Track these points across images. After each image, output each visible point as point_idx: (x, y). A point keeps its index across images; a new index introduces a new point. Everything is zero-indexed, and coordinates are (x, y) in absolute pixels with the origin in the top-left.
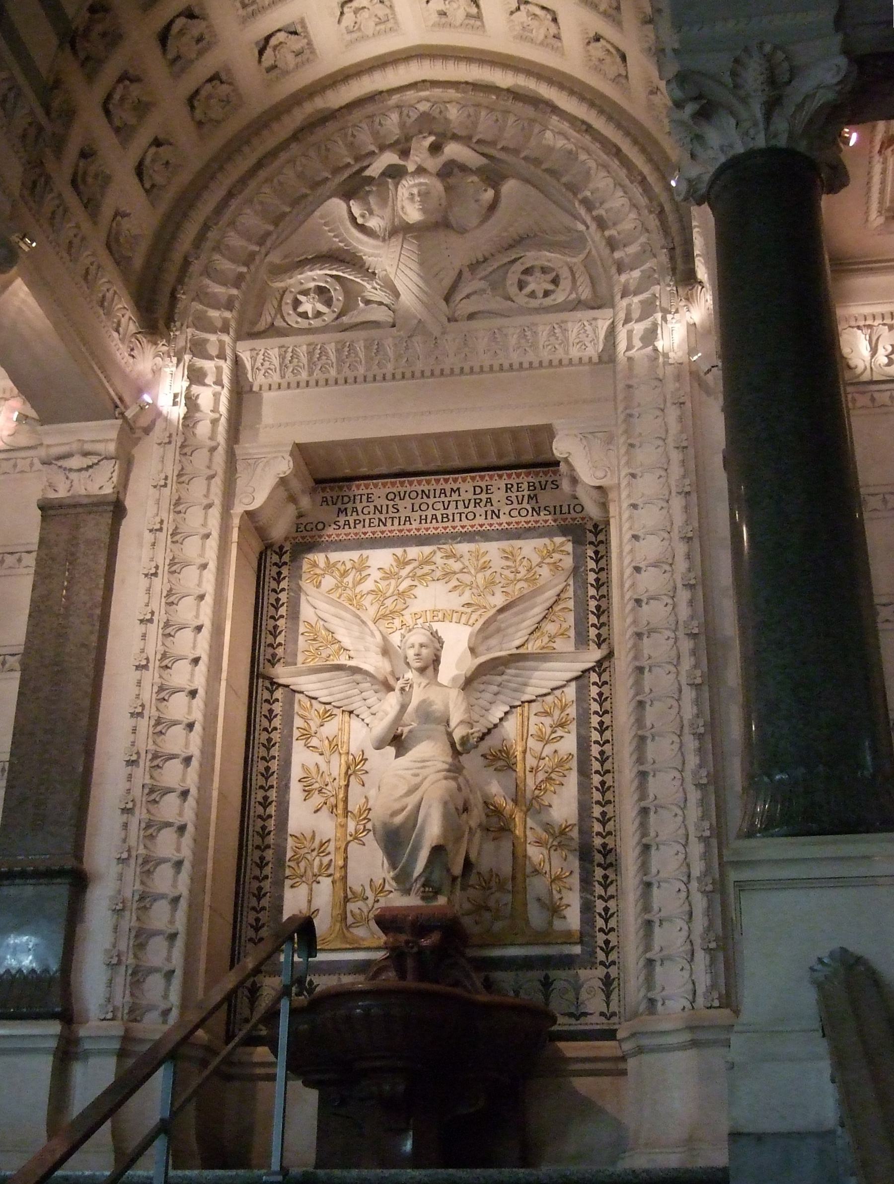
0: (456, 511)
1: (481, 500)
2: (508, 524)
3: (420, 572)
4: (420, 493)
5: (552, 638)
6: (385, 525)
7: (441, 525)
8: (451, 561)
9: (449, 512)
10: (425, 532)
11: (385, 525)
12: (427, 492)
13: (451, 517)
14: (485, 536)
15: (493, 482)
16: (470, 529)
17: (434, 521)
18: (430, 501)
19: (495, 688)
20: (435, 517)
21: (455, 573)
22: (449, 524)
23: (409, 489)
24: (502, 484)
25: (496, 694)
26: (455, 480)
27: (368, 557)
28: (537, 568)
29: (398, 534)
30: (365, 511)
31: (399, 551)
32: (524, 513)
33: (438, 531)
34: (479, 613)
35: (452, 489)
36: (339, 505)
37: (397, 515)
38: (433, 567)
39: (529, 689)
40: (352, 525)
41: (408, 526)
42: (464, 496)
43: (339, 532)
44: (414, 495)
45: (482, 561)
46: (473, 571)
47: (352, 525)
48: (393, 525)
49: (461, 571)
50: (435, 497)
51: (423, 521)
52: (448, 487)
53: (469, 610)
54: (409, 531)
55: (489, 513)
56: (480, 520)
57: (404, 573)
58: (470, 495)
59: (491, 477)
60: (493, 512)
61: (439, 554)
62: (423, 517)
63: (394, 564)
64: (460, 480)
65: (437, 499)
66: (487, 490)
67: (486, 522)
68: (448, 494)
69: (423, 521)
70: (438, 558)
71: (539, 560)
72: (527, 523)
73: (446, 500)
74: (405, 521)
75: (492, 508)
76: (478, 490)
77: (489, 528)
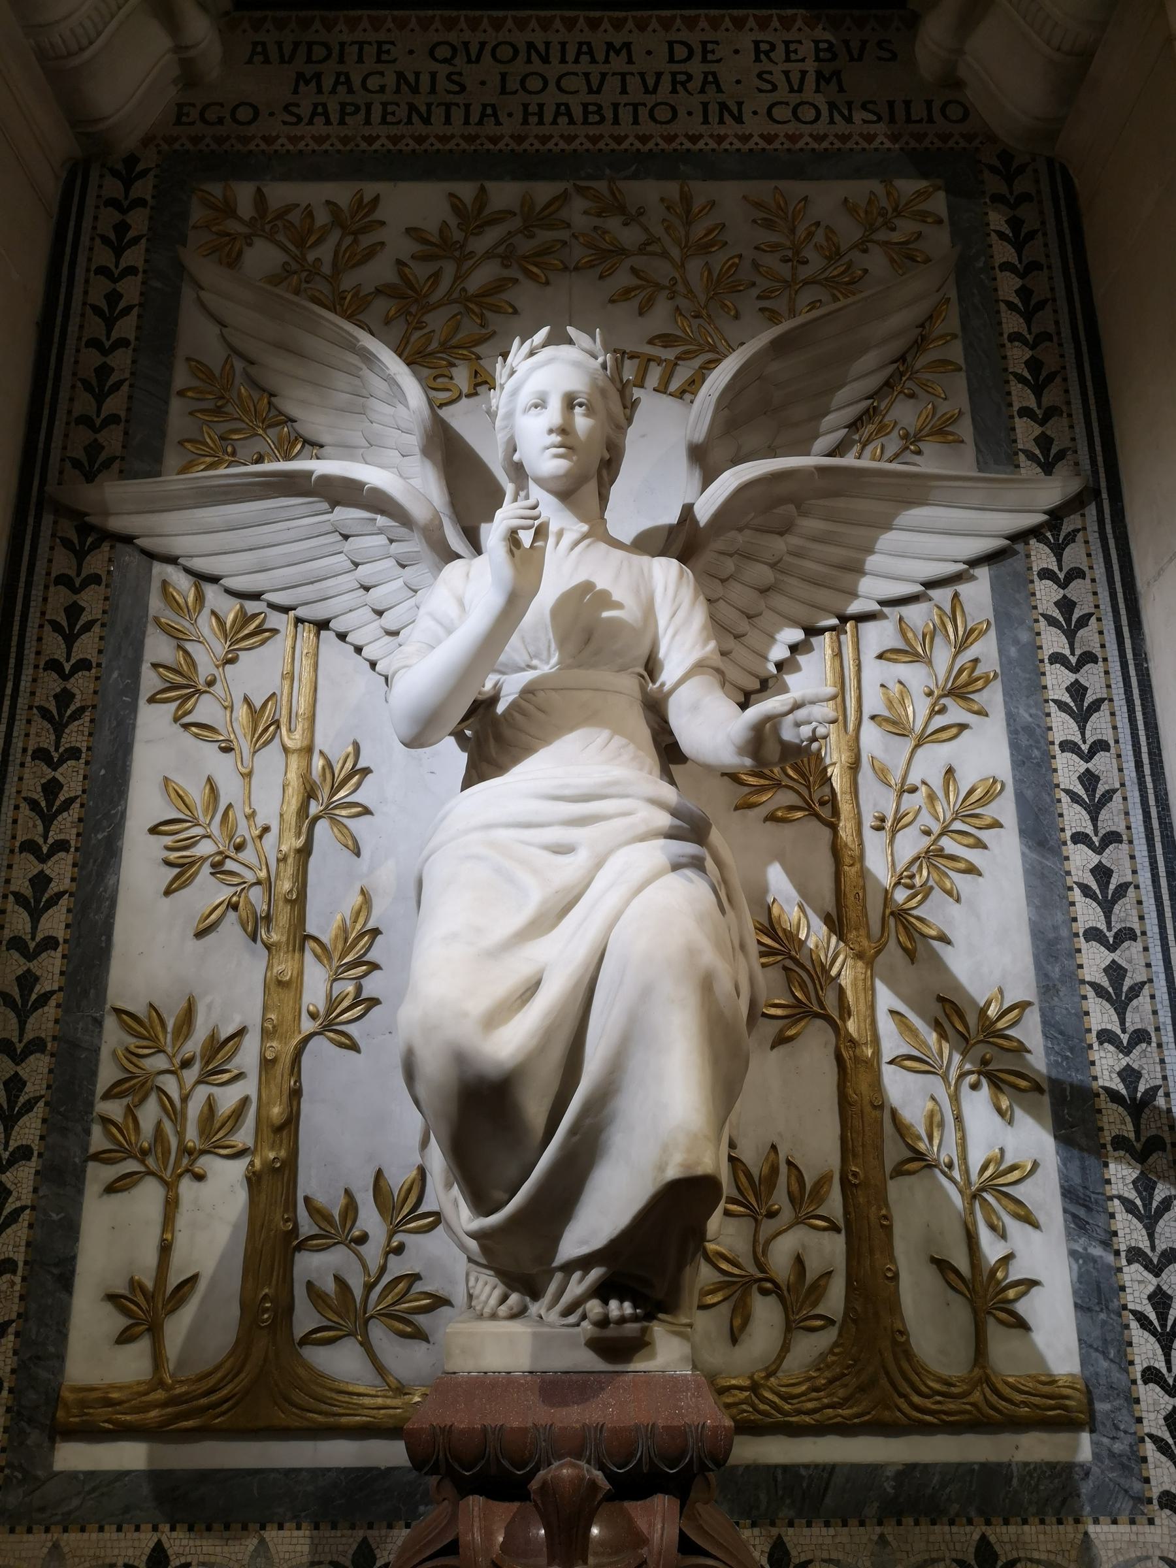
0: (624, 99)
1: (690, 77)
2: (769, 139)
3: (526, 246)
4: (523, 49)
6: (426, 121)
8: (613, 224)
10: (537, 145)
11: (426, 121)
12: (541, 48)
13: (609, 115)
16: (663, 145)
17: (563, 120)
18: (554, 69)
24: (745, 41)
26: (618, 25)
27: (376, 200)
28: (856, 255)
29: (464, 145)
30: (373, 83)
31: (466, 190)
32: (808, 114)
33: (575, 145)
34: (697, 362)
35: (610, 45)
38: (564, 235)
40: (334, 117)
43: (297, 131)
44: (505, 52)
46: (675, 253)
47: (334, 117)
48: (448, 121)
49: (642, 249)
50: (563, 61)
51: (534, 119)
53: (669, 354)
54: (494, 140)
55: (713, 109)
57: (482, 243)
59: (715, 24)
60: (723, 106)
61: (579, 204)
62: (533, 108)
63: (453, 222)
65: (571, 67)
66: (705, 52)
67: (703, 129)
68: (600, 56)
69: (534, 119)
70: (578, 213)
72: (819, 139)
74: (483, 115)
75: (721, 97)
76: (681, 52)
77: (713, 145)
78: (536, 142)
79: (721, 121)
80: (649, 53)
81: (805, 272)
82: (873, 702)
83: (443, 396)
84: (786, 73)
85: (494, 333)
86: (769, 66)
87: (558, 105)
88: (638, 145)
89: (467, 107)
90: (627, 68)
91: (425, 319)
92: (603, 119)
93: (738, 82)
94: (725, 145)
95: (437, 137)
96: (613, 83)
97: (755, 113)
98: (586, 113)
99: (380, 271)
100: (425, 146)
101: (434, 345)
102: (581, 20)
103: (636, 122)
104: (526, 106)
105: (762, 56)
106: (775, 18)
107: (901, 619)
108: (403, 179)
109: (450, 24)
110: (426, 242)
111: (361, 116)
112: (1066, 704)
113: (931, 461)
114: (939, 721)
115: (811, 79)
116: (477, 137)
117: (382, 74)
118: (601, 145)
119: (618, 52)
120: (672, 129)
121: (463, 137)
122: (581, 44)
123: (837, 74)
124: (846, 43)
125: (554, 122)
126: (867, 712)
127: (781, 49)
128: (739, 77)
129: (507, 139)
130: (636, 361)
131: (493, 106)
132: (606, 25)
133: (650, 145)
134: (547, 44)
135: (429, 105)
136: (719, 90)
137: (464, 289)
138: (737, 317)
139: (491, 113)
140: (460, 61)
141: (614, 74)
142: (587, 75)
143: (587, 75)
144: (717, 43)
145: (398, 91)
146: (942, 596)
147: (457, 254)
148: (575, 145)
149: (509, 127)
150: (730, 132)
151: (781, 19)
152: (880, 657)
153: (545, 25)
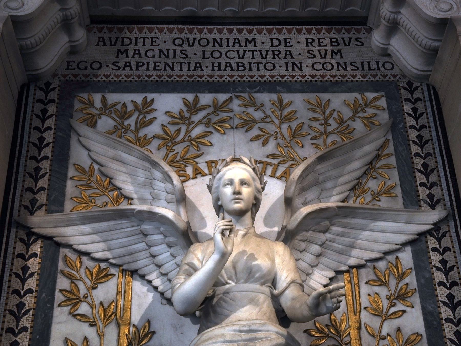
1: (280, 52)
2: (313, 77)
3: (215, 119)
4: (211, 41)
5: (376, 196)
6: (172, 69)
7: (236, 73)
8: (251, 110)
10: (218, 79)
11: (172, 69)
12: (219, 41)
13: (247, 67)
15: (292, 36)
16: (270, 79)
17: (229, 69)
18: (224, 49)
19: (315, 248)
20: (228, 65)
21: (256, 122)
22: (246, 73)
23: (198, 36)
25: (318, 256)
26: (250, 32)
27: (153, 100)
28: (350, 122)
29: (188, 79)
30: (150, 54)
31: (190, 97)
33: (234, 79)
34: (287, 165)
35: (247, 40)
36: (119, 46)
37: (186, 61)
38: (230, 114)
39: (356, 252)
40: (134, 67)
41: (199, 72)
42: (260, 46)
43: (118, 73)
44: (204, 42)
45: (286, 111)
46: (277, 122)
47: (134, 67)
48: (181, 69)
49: (263, 120)
50: (228, 46)
51: (216, 69)
52: (242, 37)
53: (275, 162)
54: (201, 77)
55: (290, 64)
56: (283, 71)
57: (196, 118)
58: (267, 46)
59: (289, 31)
60: (294, 64)
61: (236, 103)
62: (216, 64)
63: (185, 109)
64: (255, 31)
67: (286, 73)
68: (243, 44)
69: (216, 69)
70: (236, 105)
71: (351, 114)
73: (241, 50)
74: (196, 67)
75: (293, 60)
76: (276, 42)
77: (290, 79)
78: (218, 78)
79: (293, 70)
80: (263, 43)
81: (330, 129)
82: (365, 302)
83: (183, 178)
84: (319, 51)
85: (203, 153)
86: (312, 48)
87: (227, 63)
88: (259, 79)
89: (189, 63)
91: (174, 148)
92: (245, 69)
93: (300, 54)
94: (295, 79)
95: (177, 75)
97: (307, 66)
98: (238, 66)
100: (172, 79)
101: (178, 158)
102: (235, 30)
103: (258, 70)
104: (213, 64)
105: (309, 44)
106: (314, 29)
107: (375, 268)
108: (164, 92)
109: (181, 31)
111: (145, 67)
112: (446, 303)
113: (384, 202)
114: (393, 310)
115: (329, 53)
116: (194, 75)
117: (153, 50)
118: (244, 79)
119: (250, 42)
120: (273, 73)
121: (187, 75)
122: (235, 39)
123: (340, 51)
124: (343, 39)
125: (225, 70)
126: (363, 306)
127: (316, 41)
128: (300, 52)
129: (206, 77)
130: (262, 164)
131: (200, 63)
132: (245, 31)
133: (265, 79)
134: (221, 39)
135: (173, 63)
136: (292, 57)
137: (190, 136)
139: (199, 66)
140: (185, 45)
141: (249, 51)
142: (238, 51)
143: (238, 51)
144: (291, 39)
145: (160, 57)
146: (391, 258)
147: (187, 122)
148: (234, 79)
149: (207, 72)
150: (297, 74)
152: (367, 283)
153: (220, 31)
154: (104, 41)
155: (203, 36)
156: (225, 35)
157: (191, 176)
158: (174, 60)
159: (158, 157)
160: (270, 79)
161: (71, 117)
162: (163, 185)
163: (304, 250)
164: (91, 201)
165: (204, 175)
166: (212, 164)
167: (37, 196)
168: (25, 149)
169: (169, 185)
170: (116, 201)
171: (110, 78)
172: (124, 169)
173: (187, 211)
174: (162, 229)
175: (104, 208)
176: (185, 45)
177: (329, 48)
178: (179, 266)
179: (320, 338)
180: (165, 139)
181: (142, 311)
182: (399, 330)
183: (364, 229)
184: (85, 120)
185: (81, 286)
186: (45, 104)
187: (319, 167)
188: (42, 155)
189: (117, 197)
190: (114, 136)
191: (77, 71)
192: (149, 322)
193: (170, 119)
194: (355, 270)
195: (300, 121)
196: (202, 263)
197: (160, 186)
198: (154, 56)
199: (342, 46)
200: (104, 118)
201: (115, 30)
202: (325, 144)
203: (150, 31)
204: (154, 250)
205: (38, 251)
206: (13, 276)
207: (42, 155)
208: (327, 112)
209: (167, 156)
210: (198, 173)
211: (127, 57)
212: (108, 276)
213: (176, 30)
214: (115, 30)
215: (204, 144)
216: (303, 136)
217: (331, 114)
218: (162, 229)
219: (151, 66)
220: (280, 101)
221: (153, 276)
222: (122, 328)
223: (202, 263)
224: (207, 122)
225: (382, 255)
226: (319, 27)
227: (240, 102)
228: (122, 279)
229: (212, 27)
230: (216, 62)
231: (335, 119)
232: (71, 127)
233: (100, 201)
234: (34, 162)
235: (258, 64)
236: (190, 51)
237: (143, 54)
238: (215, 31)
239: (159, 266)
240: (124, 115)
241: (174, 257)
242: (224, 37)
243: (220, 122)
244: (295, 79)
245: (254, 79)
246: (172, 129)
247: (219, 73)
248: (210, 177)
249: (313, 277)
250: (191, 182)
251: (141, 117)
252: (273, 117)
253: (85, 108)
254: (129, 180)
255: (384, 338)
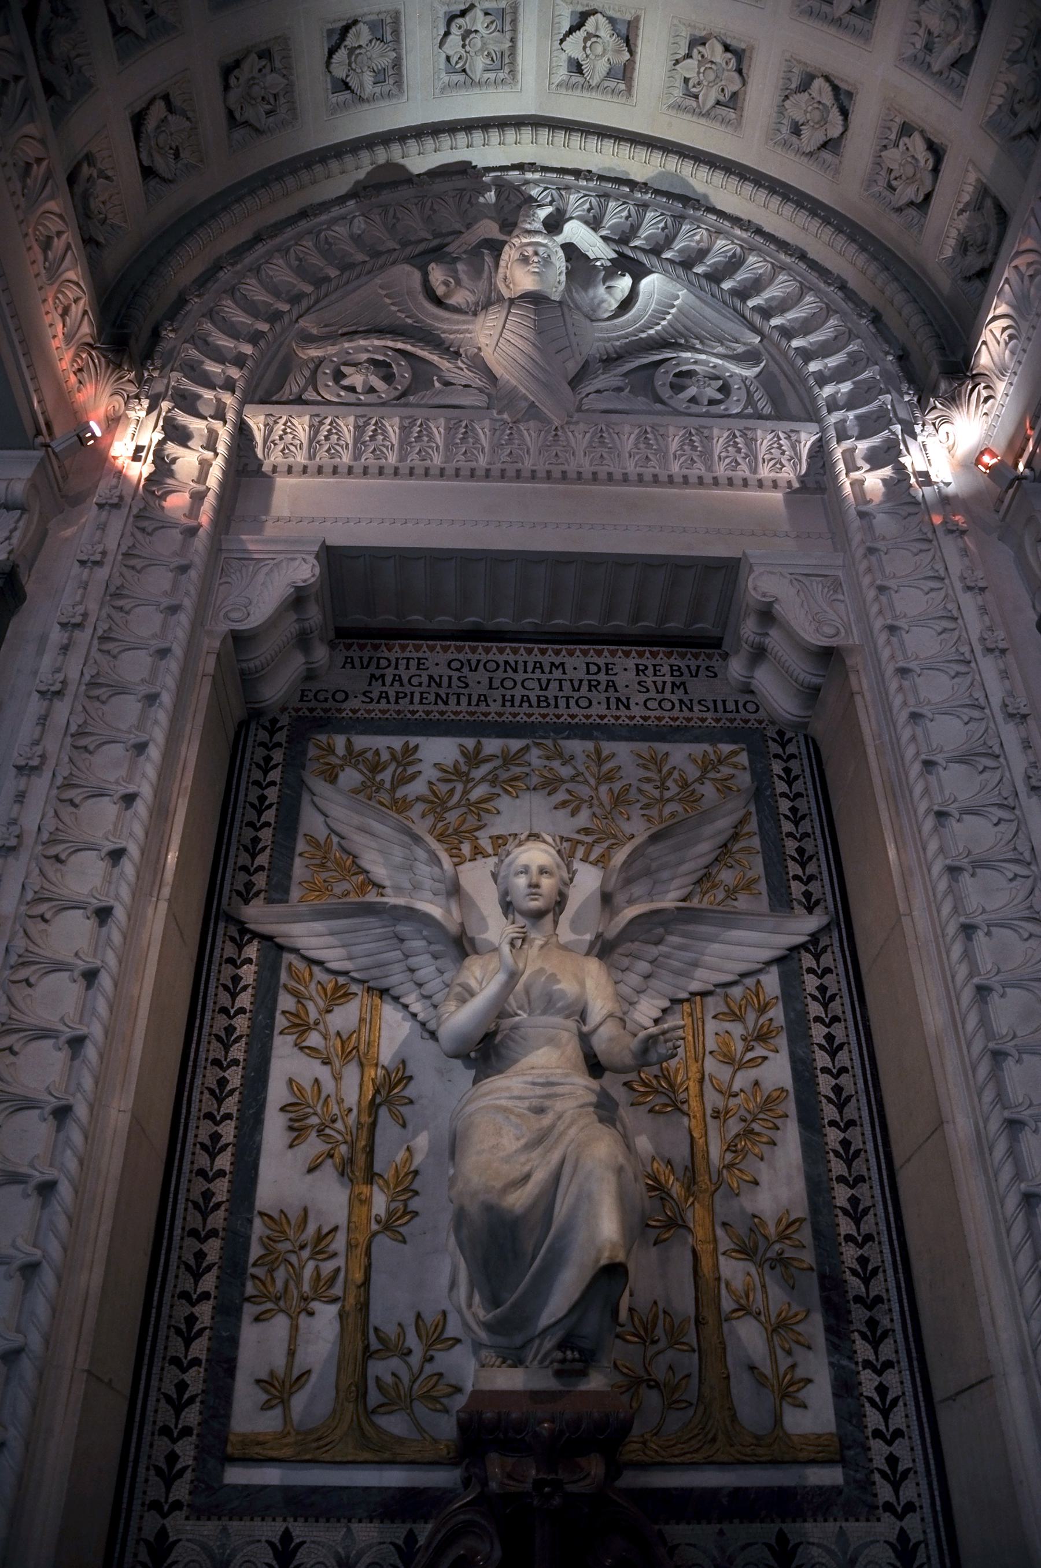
1: (599, 683)
2: (645, 719)
3: (504, 775)
4: (502, 664)
5: (731, 893)
6: (446, 703)
7: (536, 711)
8: (556, 764)
9: (550, 693)
10: (511, 718)
11: (446, 703)
12: (513, 664)
14: (611, 733)
15: (616, 660)
16: (584, 720)
18: (520, 677)
19: (644, 966)
21: (563, 781)
22: (551, 711)
23: (484, 658)
24: (631, 663)
25: (647, 977)
26: (557, 653)
27: (417, 747)
28: (696, 786)
29: (468, 717)
30: (414, 681)
31: (470, 743)
33: (533, 719)
34: (606, 845)
35: (553, 664)
37: (466, 691)
38: (526, 770)
39: (699, 973)
40: (392, 699)
41: (483, 708)
42: (571, 674)
43: (370, 707)
44: (492, 666)
45: (607, 767)
46: (592, 782)
47: (392, 699)
48: (458, 703)
49: (573, 779)
50: (525, 671)
51: (508, 704)
52: (546, 660)
53: (589, 839)
54: (486, 715)
55: (613, 701)
56: (602, 710)
57: (478, 773)
58: (582, 674)
60: (618, 700)
61: (535, 752)
62: (508, 698)
63: (462, 760)
64: (564, 652)
66: (607, 669)
67: (607, 712)
68: (547, 669)
69: (508, 704)
71: (698, 774)
73: (544, 678)
74: (479, 700)
75: (617, 695)
76: (593, 669)
77: (613, 721)
79: (618, 708)
81: (668, 794)
82: (711, 1044)
83: (456, 860)
84: (655, 682)
86: (643, 678)
89: (470, 695)
90: (564, 677)
92: (549, 705)
94: (620, 721)
96: (554, 685)
98: (539, 701)
99: (417, 788)
101: (450, 831)
103: (568, 707)
104: (504, 696)
107: (726, 996)
108: (433, 735)
109: (460, 649)
110: (446, 771)
113: (743, 902)
114: (750, 1055)
115: (668, 686)
118: (548, 719)
120: (589, 712)
123: (683, 684)
124: (688, 667)
126: (708, 1049)
127: (651, 669)
132: (550, 652)
133: (577, 720)
134: (516, 662)
135: (447, 694)
136: (616, 691)
138: (628, 819)
139: (483, 699)
140: (465, 670)
142: (539, 680)
143: (539, 680)
145: (429, 686)
146: (750, 982)
148: (533, 719)
149: (495, 707)
151: (651, 652)
152: (714, 1017)
153: (515, 651)
154: (352, 662)
155: (490, 656)
156: (522, 656)
157: (468, 857)
158: (449, 691)
159: (421, 828)
160: (584, 720)
161: (303, 767)
162: (428, 869)
163: (627, 969)
164: (326, 888)
165: (487, 856)
166: (500, 842)
167: (253, 878)
168: (239, 811)
169: (437, 869)
170: (362, 889)
171: (358, 715)
172: (373, 845)
173: (461, 906)
174: (425, 933)
175: (344, 900)
176: (465, 670)
177: (668, 679)
178: (448, 986)
179: (645, 1094)
180: (432, 802)
181: (395, 1047)
182: (756, 1083)
183: (713, 939)
184: (322, 772)
185: (311, 1006)
186: (269, 749)
187: (651, 849)
188: (263, 820)
189: (363, 883)
190: (360, 797)
191: (313, 704)
192: (404, 1062)
193: (440, 775)
194: (698, 998)
195: (625, 782)
196: (481, 984)
197: (424, 870)
198: (420, 684)
199: (686, 677)
200: (348, 769)
201: (369, 647)
202: (661, 816)
203: (417, 648)
204: (413, 961)
205: (254, 956)
206: (221, 988)
207: (263, 820)
208: (665, 770)
209: (434, 826)
210: (478, 852)
211: (384, 685)
212: (348, 995)
213: (452, 649)
214: (369, 647)
215: (488, 811)
216: (629, 803)
217: (670, 773)
218: (425, 933)
219: (417, 698)
220: (598, 752)
221: (411, 999)
222: (366, 1069)
223: (481, 984)
224: (493, 780)
225: (737, 978)
226: (655, 649)
227: (540, 752)
228: (367, 1000)
229: (503, 645)
230: (508, 694)
231: (675, 781)
232: (303, 781)
233: (339, 888)
234: (250, 829)
235: (568, 698)
236: (472, 677)
237: (405, 680)
238: (508, 650)
239: (420, 985)
240: (376, 767)
241: (441, 972)
242: (521, 659)
243: (512, 780)
244: (620, 721)
245: (562, 720)
246: (443, 788)
247: (512, 710)
248: (495, 859)
249: (638, 1006)
250: (468, 865)
251: (400, 769)
252: (587, 774)
253: (323, 756)
254: (381, 860)
255: (736, 1095)
